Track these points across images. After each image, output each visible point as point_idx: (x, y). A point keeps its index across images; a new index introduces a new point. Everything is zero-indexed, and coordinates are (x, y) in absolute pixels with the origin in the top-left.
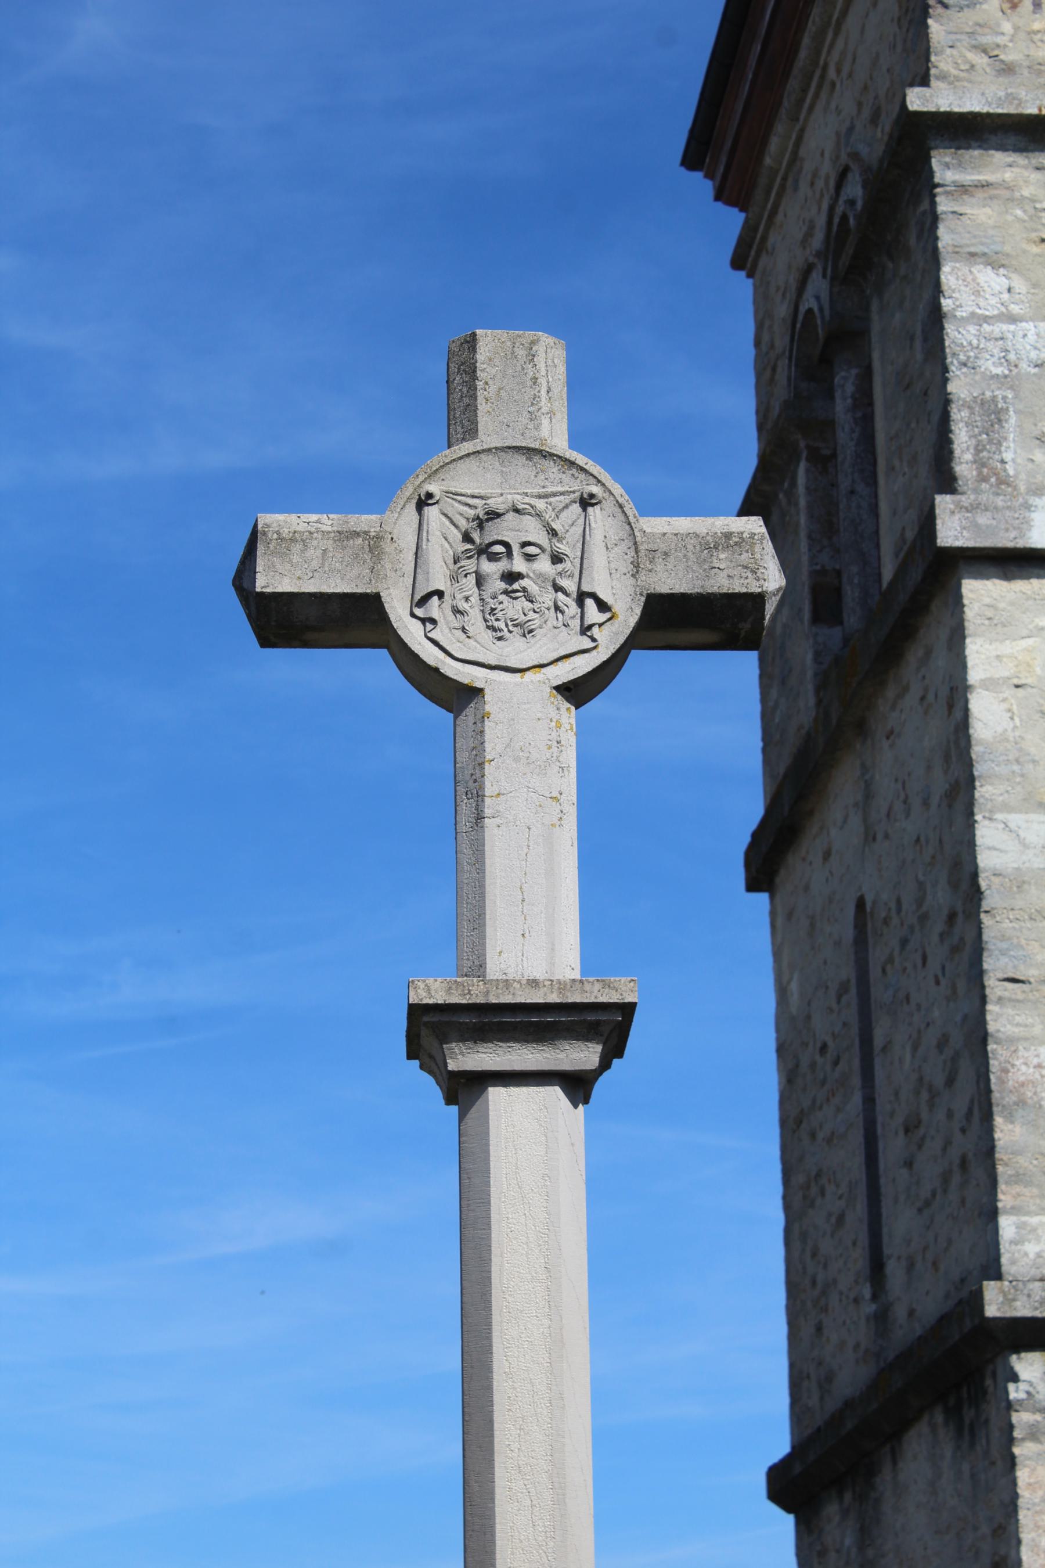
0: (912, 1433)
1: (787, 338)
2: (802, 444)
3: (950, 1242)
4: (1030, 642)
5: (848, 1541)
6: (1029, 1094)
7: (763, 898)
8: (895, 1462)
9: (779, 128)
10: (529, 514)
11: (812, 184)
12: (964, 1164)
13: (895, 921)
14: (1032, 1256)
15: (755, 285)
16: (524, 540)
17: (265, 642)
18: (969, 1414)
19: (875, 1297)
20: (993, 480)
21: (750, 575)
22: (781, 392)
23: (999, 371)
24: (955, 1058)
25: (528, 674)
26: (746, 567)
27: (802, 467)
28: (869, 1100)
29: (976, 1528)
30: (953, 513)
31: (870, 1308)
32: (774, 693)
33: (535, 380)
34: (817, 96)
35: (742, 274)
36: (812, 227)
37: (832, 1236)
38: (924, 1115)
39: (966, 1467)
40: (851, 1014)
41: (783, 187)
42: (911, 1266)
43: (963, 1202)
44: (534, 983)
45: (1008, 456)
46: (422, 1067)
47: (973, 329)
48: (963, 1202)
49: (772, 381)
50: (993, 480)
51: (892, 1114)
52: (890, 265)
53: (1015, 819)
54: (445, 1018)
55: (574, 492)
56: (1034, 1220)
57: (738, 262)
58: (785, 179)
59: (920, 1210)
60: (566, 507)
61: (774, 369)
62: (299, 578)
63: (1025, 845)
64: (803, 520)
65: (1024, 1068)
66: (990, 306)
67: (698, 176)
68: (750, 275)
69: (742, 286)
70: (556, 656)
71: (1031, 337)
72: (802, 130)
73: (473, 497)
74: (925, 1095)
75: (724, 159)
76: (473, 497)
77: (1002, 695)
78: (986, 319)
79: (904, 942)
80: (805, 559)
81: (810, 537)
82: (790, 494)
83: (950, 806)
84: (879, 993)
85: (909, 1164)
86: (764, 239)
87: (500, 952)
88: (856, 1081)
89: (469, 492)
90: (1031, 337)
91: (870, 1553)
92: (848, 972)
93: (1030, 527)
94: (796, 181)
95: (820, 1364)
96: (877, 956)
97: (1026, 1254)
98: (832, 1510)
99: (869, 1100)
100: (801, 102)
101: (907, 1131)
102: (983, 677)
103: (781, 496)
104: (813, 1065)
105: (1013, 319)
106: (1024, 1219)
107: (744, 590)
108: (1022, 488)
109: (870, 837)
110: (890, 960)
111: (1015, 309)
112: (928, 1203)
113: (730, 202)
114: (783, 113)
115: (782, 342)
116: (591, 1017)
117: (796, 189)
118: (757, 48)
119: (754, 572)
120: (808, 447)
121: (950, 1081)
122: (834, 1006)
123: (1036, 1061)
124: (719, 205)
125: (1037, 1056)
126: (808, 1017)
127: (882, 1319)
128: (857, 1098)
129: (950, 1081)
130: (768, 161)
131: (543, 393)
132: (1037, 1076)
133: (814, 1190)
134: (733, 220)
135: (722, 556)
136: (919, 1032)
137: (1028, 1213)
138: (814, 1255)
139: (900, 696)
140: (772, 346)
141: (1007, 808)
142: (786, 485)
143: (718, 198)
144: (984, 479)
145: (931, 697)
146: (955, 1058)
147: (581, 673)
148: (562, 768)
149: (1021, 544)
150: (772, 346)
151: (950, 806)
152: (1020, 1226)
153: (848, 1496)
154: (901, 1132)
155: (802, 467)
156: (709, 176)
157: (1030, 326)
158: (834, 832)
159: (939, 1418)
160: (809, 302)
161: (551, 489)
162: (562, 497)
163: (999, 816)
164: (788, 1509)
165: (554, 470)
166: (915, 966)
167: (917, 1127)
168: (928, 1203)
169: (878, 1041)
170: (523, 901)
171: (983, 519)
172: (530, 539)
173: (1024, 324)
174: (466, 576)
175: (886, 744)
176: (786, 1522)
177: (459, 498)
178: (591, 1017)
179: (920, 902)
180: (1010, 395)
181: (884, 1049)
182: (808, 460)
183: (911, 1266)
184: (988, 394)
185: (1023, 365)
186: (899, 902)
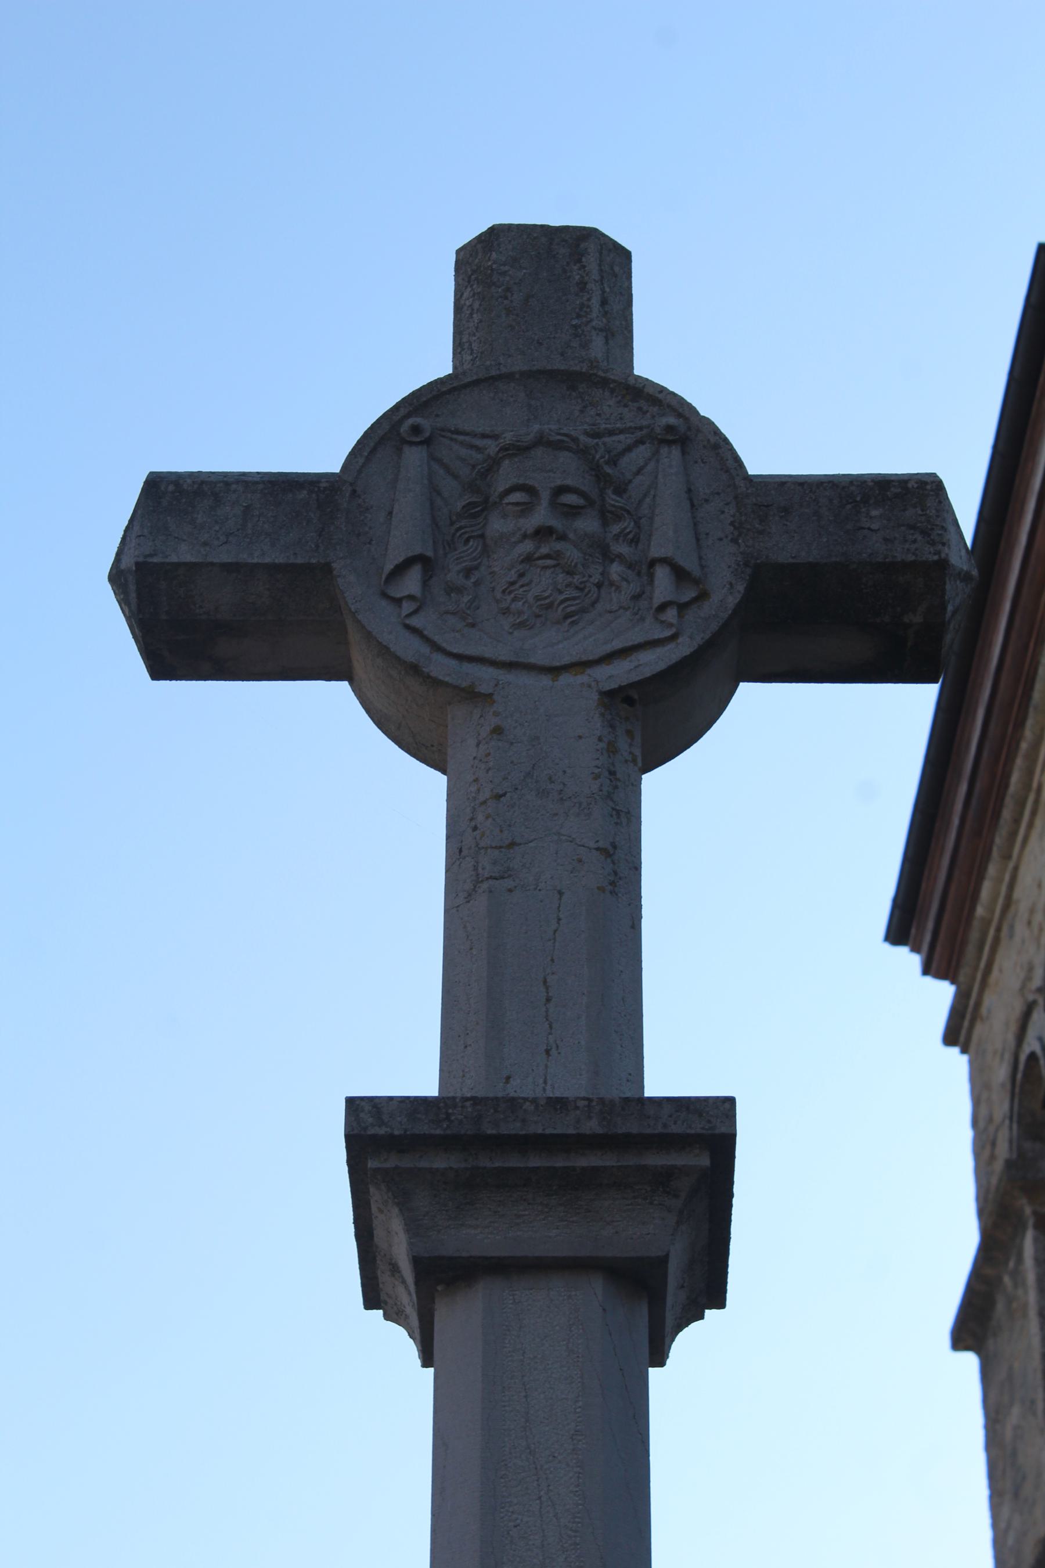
1: (1006, 1106)
2: (1028, 1210)
9: (992, 870)
10: (568, 449)
11: (1029, 923)
15: (971, 1063)
16: (559, 482)
17: (157, 673)
21: (919, 537)
22: (1003, 1150)
25: (565, 679)
26: (912, 527)
32: (1006, 1511)
33: (582, 286)
34: (1031, 825)
35: (955, 1051)
36: (1031, 969)
41: (997, 941)
44: (559, 1104)
46: (387, 1317)
49: (992, 1157)
54: (406, 1162)
55: (641, 428)
57: (951, 1037)
58: (999, 929)
60: (629, 449)
61: (994, 1144)
62: (205, 544)
67: (903, 951)
68: (964, 1051)
69: (957, 1062)
70: (608, 648)
72: (1016, 869)
73: (484, 436)
75: (930, 925)
76: (484, 436)
82: (1017, 1275)
86: (978, 1004)
87: (508, 1078)
94: (1012, 927)
100: (1013, 834)
103: (1007, 1280)
107: (911, 558)
113: (940, 975)
114: (995, 853)
115: (1001, 1108)
116: (655, 1160)
117: (1011, 936)
118: (963, 788)
119: (925, 533)
120: (1035, 1213)
124: (929, 980)
130: (980, 911)
131: (595, 302)
134: (943, 993)
135: (874, 513)
140: (990, 1120)
142: (1011, 1264)
143: (926, 971)
147: (647, 672)
148: (618, 812)
150: (990, 1120)
156: (915, 949)
162: (622, 437)
165: (611, 402)
172: (569, 482)
174: (467, 541)
177: (461, 438)
178: (655, 1160)
182: (1036, 1227)
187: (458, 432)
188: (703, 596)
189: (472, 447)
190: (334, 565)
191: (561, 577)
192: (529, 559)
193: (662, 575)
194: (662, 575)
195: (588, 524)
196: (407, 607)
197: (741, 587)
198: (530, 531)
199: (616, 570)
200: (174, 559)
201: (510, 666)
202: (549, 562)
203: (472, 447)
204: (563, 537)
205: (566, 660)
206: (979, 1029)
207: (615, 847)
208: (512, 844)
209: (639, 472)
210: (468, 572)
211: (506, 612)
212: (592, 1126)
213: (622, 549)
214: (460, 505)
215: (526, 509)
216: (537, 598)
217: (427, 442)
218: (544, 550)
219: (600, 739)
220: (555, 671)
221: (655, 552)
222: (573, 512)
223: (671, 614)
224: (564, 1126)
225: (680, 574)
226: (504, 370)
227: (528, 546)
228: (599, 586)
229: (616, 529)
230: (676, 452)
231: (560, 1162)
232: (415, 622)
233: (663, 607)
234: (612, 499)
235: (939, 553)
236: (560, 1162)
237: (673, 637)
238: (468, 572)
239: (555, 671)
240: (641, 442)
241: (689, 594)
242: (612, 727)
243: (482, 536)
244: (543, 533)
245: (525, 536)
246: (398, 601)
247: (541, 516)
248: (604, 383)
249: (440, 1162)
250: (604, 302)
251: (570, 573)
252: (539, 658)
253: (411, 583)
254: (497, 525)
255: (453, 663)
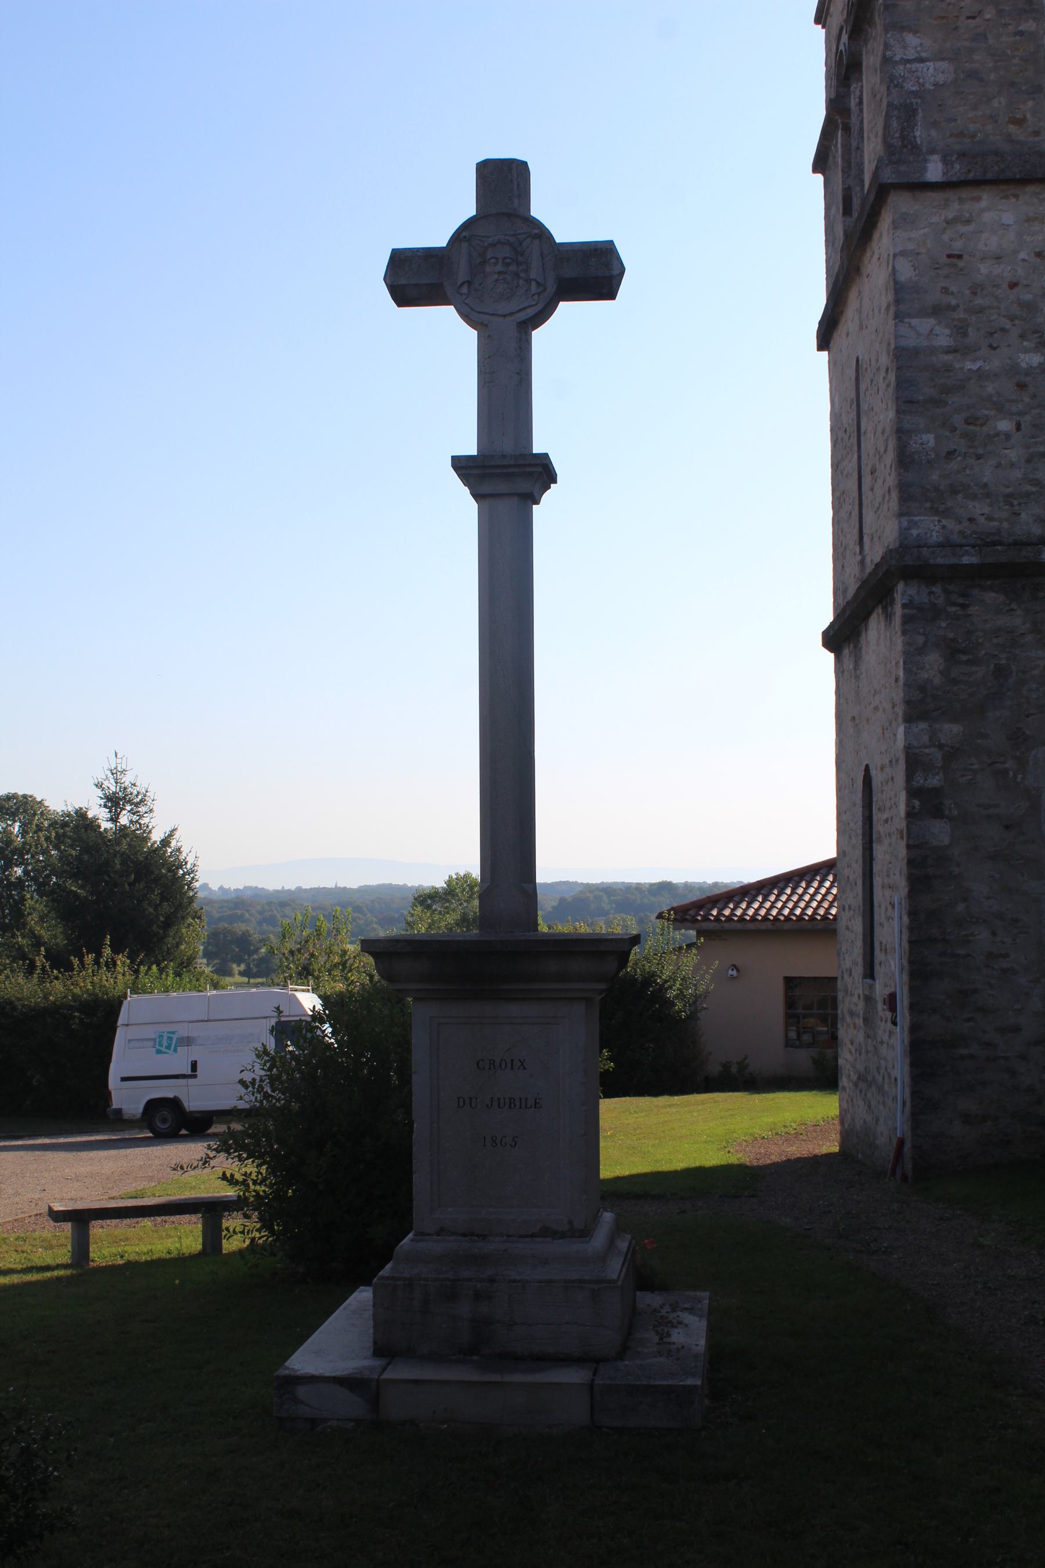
0: (872, 618)
2: (839, 121)
3: (884, 528)
4: (926, 230)
5: (851, 666)
6: (916, 458)
7: (825, 354)
8: (866, 631)
12: (889, 491)
13: (869, 370)
14: (915, 535)
18: (889, 609)
19: (860, 553)
20: (910, 146)
23: (914, 89)
24: (887, 440)
27: (840, 132)
28: (859, 457)
29: (891, 663)
30: (887, 165)
31: (859, 558)
33: (512, 180)
35: (820, 26)
37: (847, 522)
38: (877, 467)
39: (888, 634)
40: (853, 415)
42: (872, 538)
43: (889, 509)
45: (918, 134)
47: (901, 67)
48: (889, 509)
50: (910, 146)
51: (867, 465)
52: (870, 30)
53: (915, 321)
56: (917, 518)
59: (875, 512)
60: (525, 239)
63: (919, 334)
64: (840, 160)
65: (914, 445)
66: (911, 54)
68: (823, 27)
69: (820, 32)
70: (518, 309)
71: (931, 70)
74: (877, 457)
77: (910, 259)
78: (909, 61)
79: (872, 381)
80: (840, 181)
81: (843, 171)
82: (836, 146)
83: (887, 314)
84: (864, 407)
85: (872, 490)
86: (828, 8)
88: (855, 448)
89: (483, 235)
90: (931, 70)
91: (858, 672)
92: (853, 395)
93: (926, 171)
95: (843, 583)
96: (863, 387)
97: (912, 535)
98: (846, 652)
99: (859, 457)
101: (872, 473)
102: (901, 249)
103: (833, 147)
104: (842, 439)
105: (922, 60)
106: (911, 518)
108: (924, 150)
109: (861, 328)
110: (867, 390)
111: (924, 55)
112: (878, 509)
120: (842, 123)
121: (886, 451)
122: (849, 410)
123: (920, 441)
125: (921, 439)
126: (841, 415)
127: (862, 562)
128: (856, 457)
129: (886, 451)
131: (515, 187)
132: (921, 449)
133: (842, 499)
135: (593, 259)
136: (876, 425)
137: (914, 516)
138: (842, 531)
139: (872, 257)
141: (910, 316)
142: (834, 142)
144: (905, 146)
145: (881, 258)
146: (887, 440)
147: (530, 316)
149: (921, 180)
151: (887, 314)
152: (910, 521)
153: (851, 646)
154: (870, 474)
155: (840, 132)
157: (930, 64)
158: (850, 322)
159: (880, 611)
160: (842, 47)
161: (518, 232)
163: (906, 320)
164: (832, 652)
166: (875, 393)
167: (875, 472)
168: (878, 509)
169: (863, 430)
170: (503, 419)
171: (903, 168)
172: (508, 255)
173: (928, 63)
174: (480, 273)
175: (866, 280)
176: (830, 657)
177: (478, 238)
179: (877, 360)
180: (919, 101)
181: (865, 433)
182: (842, 129)
183: (872, 538)
184: (908, 101)
185: (927, 85)
186: (870, 360)
187: (478, 236)
188: (545, 289)
189: (481, 240)
190: (444, 284)
191: (506, 286)
192: (497, 280)
193: (533, 284)
194: (533, 284)
195: (513, 268)
196: (464, 297)
197: (555, 287)
198: (497, 271)
199: (521, 282)
200: (400, 283)
201: (493, 314)
202: (503, 281)
203: (481, 240)
204: (506, 273)
205: (508, 312)
206: (829, 19)
207: (521, 370)
208: (493, 372)
209: (528, 247)
210: (480, 284)
211: (491, 297)
212: (512, 462)
213: (523, 275)
214: (478, 261)
215: (496, 264)
216: (500, 293)
217: (468, 240)
218: (501, 278)
219: (517, 338)
220: (504, 316)
221: (532, 277)
222: (508, 265)
223: (536, 297)
224: (505, 462)
225: (538, 283)
226: (489, 213)
227: (496, 276)
228: (517, 287)
229: (521, 268)
230: (537, 241)
231: (505, 471)
232: (466, 301)
233: (534, 295)
234: (521, 259)
235: (610, 273)
236: (505, 471)
237: (537, 304)
238: (480, 284)
239: (504, 316)
240: (528, 237)
241: (541, 289)
242: (520, 332)
243: (484, 272)
244: (500, 273)
245: (495, 273)
246: (461, 294)
247: (499, 267)
248: (518, 216)
249: (475, 472)
250: (518, 185)
251: (508, 284)
252: (500, 312)
253: (464, 290)
254: (488, 269)
255: (477, 314)
